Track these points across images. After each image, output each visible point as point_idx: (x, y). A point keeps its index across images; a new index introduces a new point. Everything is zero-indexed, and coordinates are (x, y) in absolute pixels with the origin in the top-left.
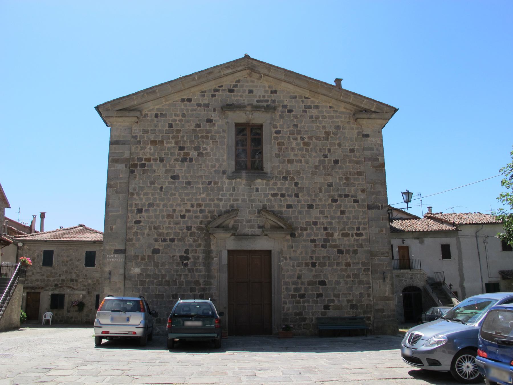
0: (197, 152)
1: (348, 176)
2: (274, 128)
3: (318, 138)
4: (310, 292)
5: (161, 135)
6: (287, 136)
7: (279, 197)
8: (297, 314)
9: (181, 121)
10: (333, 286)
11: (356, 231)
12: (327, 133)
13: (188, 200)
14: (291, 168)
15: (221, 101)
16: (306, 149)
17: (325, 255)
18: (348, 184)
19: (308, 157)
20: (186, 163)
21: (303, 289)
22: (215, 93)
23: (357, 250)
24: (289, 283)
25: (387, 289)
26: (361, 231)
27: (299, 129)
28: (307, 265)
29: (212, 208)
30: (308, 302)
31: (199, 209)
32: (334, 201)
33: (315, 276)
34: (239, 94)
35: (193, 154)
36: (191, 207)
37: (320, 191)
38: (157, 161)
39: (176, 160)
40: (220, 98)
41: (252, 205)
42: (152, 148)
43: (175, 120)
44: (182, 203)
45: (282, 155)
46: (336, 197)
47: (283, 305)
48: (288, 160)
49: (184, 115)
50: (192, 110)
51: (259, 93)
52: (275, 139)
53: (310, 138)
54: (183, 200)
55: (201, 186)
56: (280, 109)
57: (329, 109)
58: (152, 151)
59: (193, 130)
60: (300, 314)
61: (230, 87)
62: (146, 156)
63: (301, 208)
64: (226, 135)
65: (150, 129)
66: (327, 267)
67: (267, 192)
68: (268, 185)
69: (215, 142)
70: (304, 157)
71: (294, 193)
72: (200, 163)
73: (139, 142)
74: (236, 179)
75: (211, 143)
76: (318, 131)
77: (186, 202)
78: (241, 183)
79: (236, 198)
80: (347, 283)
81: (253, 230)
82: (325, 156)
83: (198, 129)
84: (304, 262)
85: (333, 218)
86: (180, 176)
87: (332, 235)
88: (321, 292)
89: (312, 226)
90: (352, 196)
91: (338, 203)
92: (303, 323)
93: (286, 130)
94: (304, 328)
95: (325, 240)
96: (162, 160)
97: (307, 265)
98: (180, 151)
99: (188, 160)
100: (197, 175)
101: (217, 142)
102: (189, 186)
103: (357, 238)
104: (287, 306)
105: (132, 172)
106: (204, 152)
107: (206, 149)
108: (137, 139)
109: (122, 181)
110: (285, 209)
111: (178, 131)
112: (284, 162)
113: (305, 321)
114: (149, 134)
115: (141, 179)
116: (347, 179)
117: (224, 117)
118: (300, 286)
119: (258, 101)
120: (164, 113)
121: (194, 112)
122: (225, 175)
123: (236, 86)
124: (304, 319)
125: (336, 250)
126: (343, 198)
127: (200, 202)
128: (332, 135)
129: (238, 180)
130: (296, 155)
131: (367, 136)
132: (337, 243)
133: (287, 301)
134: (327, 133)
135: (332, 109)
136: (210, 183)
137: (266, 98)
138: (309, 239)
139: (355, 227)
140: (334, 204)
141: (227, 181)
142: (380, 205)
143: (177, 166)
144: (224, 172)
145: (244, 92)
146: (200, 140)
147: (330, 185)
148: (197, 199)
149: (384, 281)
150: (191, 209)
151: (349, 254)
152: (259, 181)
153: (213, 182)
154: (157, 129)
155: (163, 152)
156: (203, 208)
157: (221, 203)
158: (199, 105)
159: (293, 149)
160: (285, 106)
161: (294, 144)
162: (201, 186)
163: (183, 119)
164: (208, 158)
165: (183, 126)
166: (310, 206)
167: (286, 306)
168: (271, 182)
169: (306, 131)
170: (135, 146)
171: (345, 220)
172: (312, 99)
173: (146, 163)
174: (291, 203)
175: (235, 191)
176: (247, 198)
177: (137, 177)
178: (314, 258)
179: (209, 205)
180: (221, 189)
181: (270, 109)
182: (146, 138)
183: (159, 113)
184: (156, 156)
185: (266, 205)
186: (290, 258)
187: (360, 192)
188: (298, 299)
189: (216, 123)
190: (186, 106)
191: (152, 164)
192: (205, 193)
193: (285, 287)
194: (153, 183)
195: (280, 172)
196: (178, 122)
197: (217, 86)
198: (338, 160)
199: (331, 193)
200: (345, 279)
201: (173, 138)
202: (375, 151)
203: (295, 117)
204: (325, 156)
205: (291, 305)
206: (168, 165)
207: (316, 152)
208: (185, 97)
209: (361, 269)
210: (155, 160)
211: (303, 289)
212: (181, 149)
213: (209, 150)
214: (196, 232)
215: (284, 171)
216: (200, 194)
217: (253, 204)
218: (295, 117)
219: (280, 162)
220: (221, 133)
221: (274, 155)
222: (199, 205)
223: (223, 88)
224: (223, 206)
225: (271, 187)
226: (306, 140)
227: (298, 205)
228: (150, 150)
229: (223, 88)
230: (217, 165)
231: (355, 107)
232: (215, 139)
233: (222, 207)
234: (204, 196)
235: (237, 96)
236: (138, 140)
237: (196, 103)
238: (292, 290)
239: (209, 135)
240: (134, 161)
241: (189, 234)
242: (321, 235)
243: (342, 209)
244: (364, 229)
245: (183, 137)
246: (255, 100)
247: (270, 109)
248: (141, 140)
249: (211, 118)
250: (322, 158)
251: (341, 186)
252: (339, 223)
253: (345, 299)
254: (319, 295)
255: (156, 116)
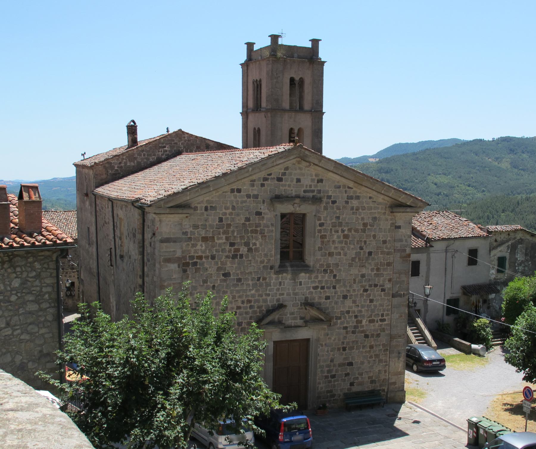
0: (246, 248)
1: (379, 267)
2: (318, 220)
3: (356, 231)
4: (340, 373)
5: (211, 230)
6: (329, 228)
7: (319, 289)
8: (328, 392)
9: (231, 214)
10: (359, 366)
11: (380, 318)
12: (365, 225)
13: (239, 297)
14: (331, 260)
15: (270, 192)
16: (345, 241)
17: (354, 340)
18: (378, 274)
19: (346, 249)
20: (236, 260)
21: (334, 370)
22: (264, 182)
23: (380, 334)
24: (324, 366)
25: (400, 365)
26: (384, 318)
27: (340, 221)
28: (339, 349)
29: (261, 304)
30: (338, 381)
31: (248, 305)
32: (366, 290)
33: (345, 359)
34: (288, 183)
35: (243, 250)
36: (242, 303)
37: (355, 282)
38: (208, 259)
39: (227, 257)
40: (269, 188)
41: (296, 298)
42: (204, 245)
43: (225, 214)
44: (233, 300)
45: (324, 248)
46: (367, 287)
47: (317, 386)
48: (329, 253)
49: (234, 208)
50: (243, 202)
51: (306, 182)
52: (318, 232)
53: (350, 230)
54: (234, 297)
55: (250, 282)
56: (325, 200)
57: (369, 200)
58: (204, 248)
59: (243, 224)
60: (331, 391)
61: (279, 175)
62: (198, 253)
63: (337, 298)
64: (274, 229)
65: (200, 224)
66: (355, 350)
67: (309, 285)
68: (310, 278)
69: (264, 236)
70: (343, 250)
71: (332, 285)
72: (250, 259)
73: (190, 239)
74: (282, 274)
75: (260, 237)
76: (357, 223)
77: (237, 299)
78: (287, 277)
79: (283, 292)
80: (369, 363)
81: (296, 321)
82: (361, 248)
83: (247, 223)
84: (336, 347)
85: (363, 306)
86: (231, 273)
87: (361, 322)
88: (348, 371)
89: (346, 314)
90: (380, 286)
91: (368, 292)
92: (332, 399)
93: (329, 222)
94: (333, 403)
95: (356, 327)
96: (213, 258)
97: (339, 349)
98: (230, 248)
99: (238, 257)
100: (247, 272)
101: (265, 236)
102: (239, 283)
103: (381, 323)
104: (321, 385)
105: (185, 271)
106: (253, 247)
107: (255, 244)
108: (187, 235)
109: (175, 282)
110: (324, 300)
111: (229, 226)
112: (325, 255)
113: (334, 397)
114: (200, 229)
115: (194, 278)
116: (378, 269)
117: (272, 209)
118: (332, 368)
119: (305, 191)
120: (213, 205)
121: (244, 204)
122: (273, 271)
123: (284, 174)
124: (334, 396)
125: (363, 334)
126: (373, 288)
127: (250, 298)
128: (369, 227)
129: (285, 274)
130: (336, 248)
131: (399, 227)
132: (365, 329)
133: (321, 381)
134: (365, 225)
135: (371, 200)
136: (259, 279)
137: (313, 188)
138: (342, 326)
139: (380, 313)
140: (365, 293)
141: (274, 276)
142: (402, 293)
143: (228, 263)
144: (272, 268)
145: (292, 181)
146: (250, 234)
147: (363, 276)
148: (247, 296)
149: (399, 359)
150: (242, 305)
151: (373, 337)
152: (303, 274)
153: (261, 278)
154: (207, 224)
155: (215, 249)
156: (252, 304)
157: (269, 298)
158: (248, 196)
159: (334, 242)
160: (329, 197)
161: (335, 237)
162: (250, 282)
163: (233, 212)
164: (257, 254)
165: (233, 220)
166: (345, 297)
167: (320, 386)
168: (313, 276)
169: (347, 223)
170: (186, 243)
171: (373, 308)
172: (354, 189)
173: (198, 261)
174: (329, 295)
175: (281, 285)
176: (292, 292)
177: (190, 276)
178: (345, 343)
179: (257, 301)
180: (268, 285)
181: (316, 200)
182: (196, 234)
183: (209, 206)
184: (208, 254)
185: (308, 297)
186: (325, 344)
187: (387, 282)
188: (330, 379)
189: (265, 216)
190: (235, 197)
191: (204, 262)
192: (255, 289)
193: (320, 370)
194: (205, 282)
195: (322, 265)
196: (228, 216)
197: (266, 174)
198: (372, 252)
199: (364, 283)
200: (369, 359)
201: (224, 233)
202: (404, 243)
203: (338, 208)
204: (361, 248)
205: (324, 385)
206: (219, 263)
207: (354, 244)
208: (235, 187)
209: (382, 349)
210: (207, 257)
211: (334, 370)
212: (232, 244)
213: (258, 246)
214: (246, 327)
215: (325, 264)
216: (250, 290)
217: (297, 297)
218: (338, 208)
219: (322, 256)
220: (269, 227)
221: (317, 249)
222: (249, 301)
223: (272, 176)
224: (271, 301)
225: (313, 280)
226: (346, 232)
227: (335, 296)
228: (201, 247)
229: (272, 176)
230: (266, 261)
231: (393, 200)
232: (264, 234)
233: (270, 302)
234: (253, 292)
235: (285, 185)
236: (189, 236)
237: (245, 194)
238: (326, 372)
239: (259, 229)
240: (186, 259)
241: (240, 330)
242: (352, 322)
243: (371, 298)
244: (387, 315)
245: (233, 232)
246: (303, 189)
248: (192, 237)
249: (261, 211)
250: (359, 250)
251: (372, 277)
252: (368, 310)
253: (367, 376)
254: (347, 375)
255: (206, 209)
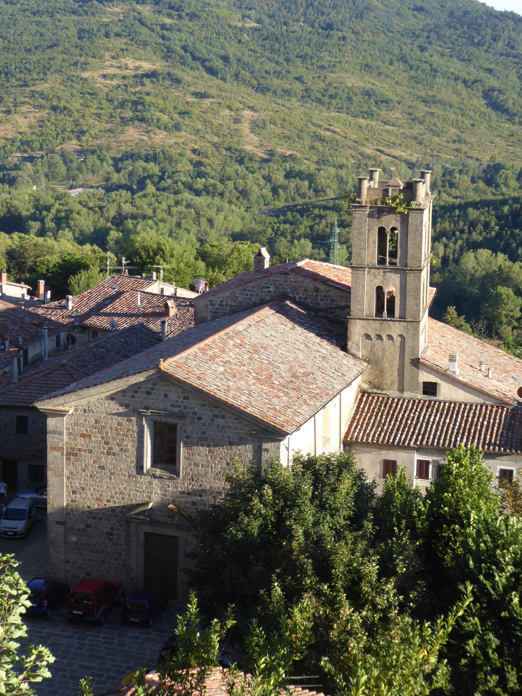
35: (116, 449)
96: (91, 452)
119: (172, 406)
123: (152, 389)
145: (160, 395)
160: (195, 413)
203: (204, 424)
210: (85, 451)
218: (204, 424)
223: (142, 390)
229: (142, 390)
235: (153, 399)
246: (170, 404)
247: (182, 416)
